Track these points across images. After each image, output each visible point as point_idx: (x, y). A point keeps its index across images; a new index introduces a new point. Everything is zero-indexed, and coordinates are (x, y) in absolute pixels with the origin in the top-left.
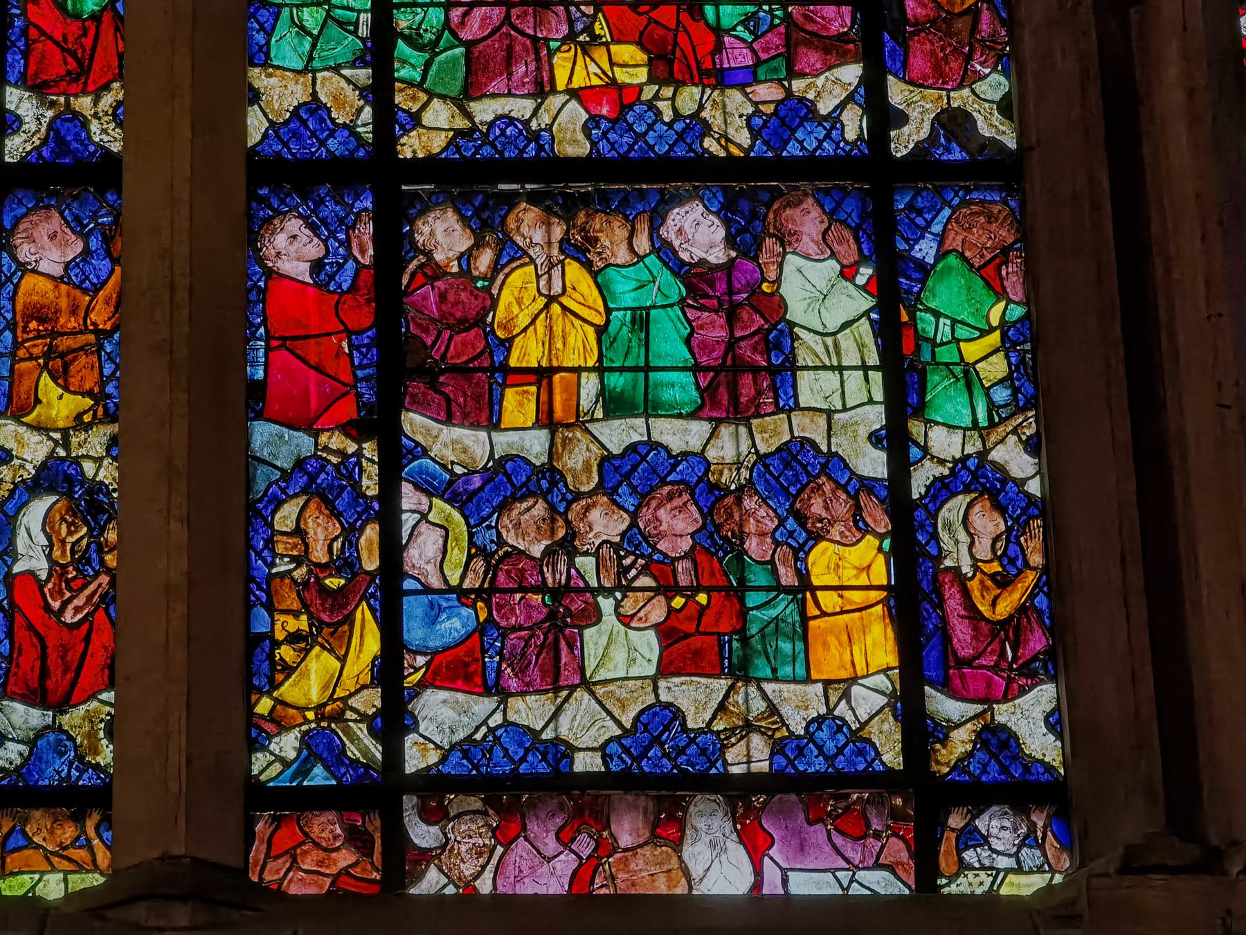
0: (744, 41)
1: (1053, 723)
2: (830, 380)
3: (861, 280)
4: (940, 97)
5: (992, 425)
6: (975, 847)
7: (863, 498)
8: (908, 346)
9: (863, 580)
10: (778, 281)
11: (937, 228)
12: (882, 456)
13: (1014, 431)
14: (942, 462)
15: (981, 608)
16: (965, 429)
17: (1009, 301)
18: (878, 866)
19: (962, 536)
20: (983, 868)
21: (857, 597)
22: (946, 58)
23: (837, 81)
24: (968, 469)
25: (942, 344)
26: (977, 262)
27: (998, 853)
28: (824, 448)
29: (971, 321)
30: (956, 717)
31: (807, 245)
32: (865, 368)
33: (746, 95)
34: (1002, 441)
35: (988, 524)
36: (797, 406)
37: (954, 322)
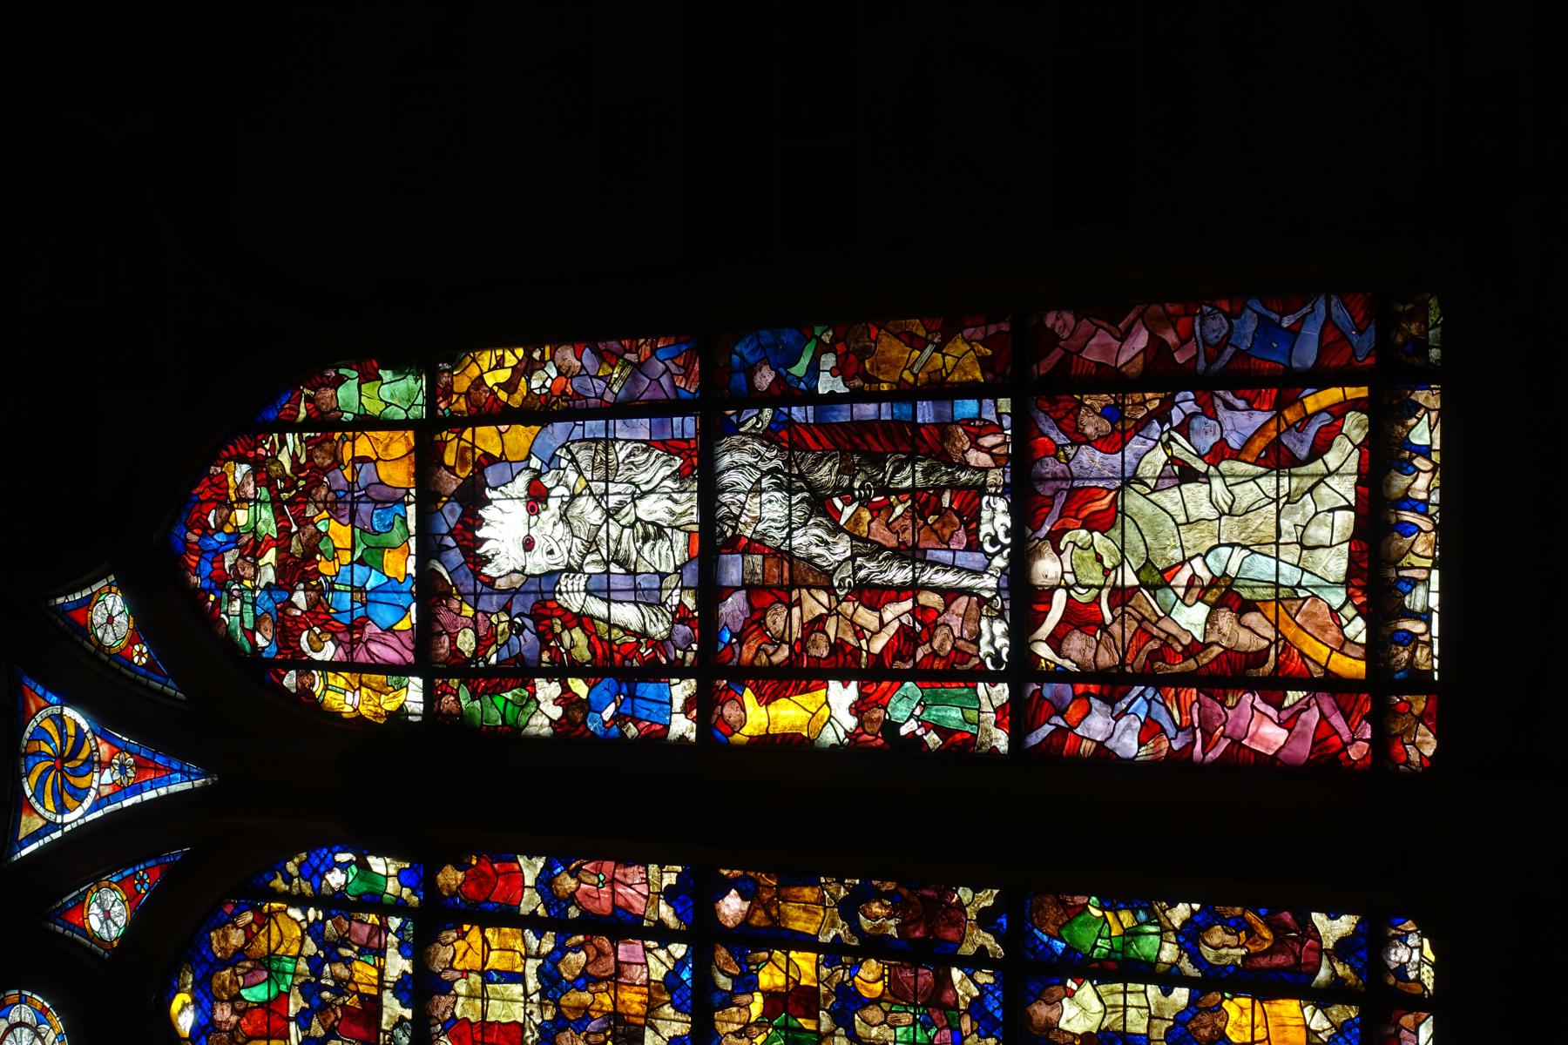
0: (936, 1033)
1: (1334, 915)
2: (1132, 1013)
3: (1074, 987)
4: (971, 925)
5: (1159, 924)
6: (1406, 972)
7: (1201, 1006)
8: (1112, 965)
9: (1249, 1012)
10: (1074, 1035)
11: (1045, 938)
12: (1176, 990)
13: (1164, 912)
14: (1180, 957)
15: (1266, 946)
16: (1162, 940)
17: (1088, 903)
18: (1416, 1033)
19: (1224, 951)
20: (1419, 969)
21: (1258, 1018)
22: (949, 919)
23: (961, 982)
24: (1184, 942)
25: (1112, 945)
26: (1066, 919)
27: (1410, 958)
28: (1171, 1023)
29: (1100, 926)
30: (1330, 972)
31: (1053, 1014)
32: (1125, 993)
33: (967, 1037)
34: (1169, 920)
35: (1217, 935)
36: (1147, 1035)
37: (1099, 936)
